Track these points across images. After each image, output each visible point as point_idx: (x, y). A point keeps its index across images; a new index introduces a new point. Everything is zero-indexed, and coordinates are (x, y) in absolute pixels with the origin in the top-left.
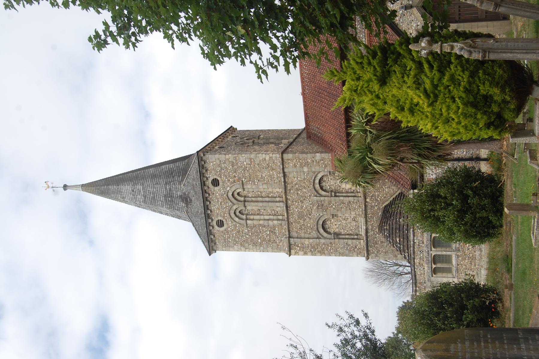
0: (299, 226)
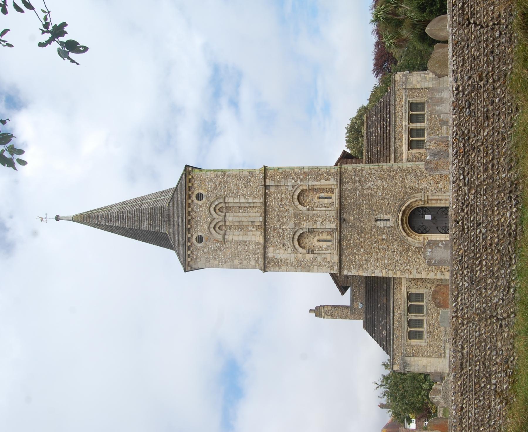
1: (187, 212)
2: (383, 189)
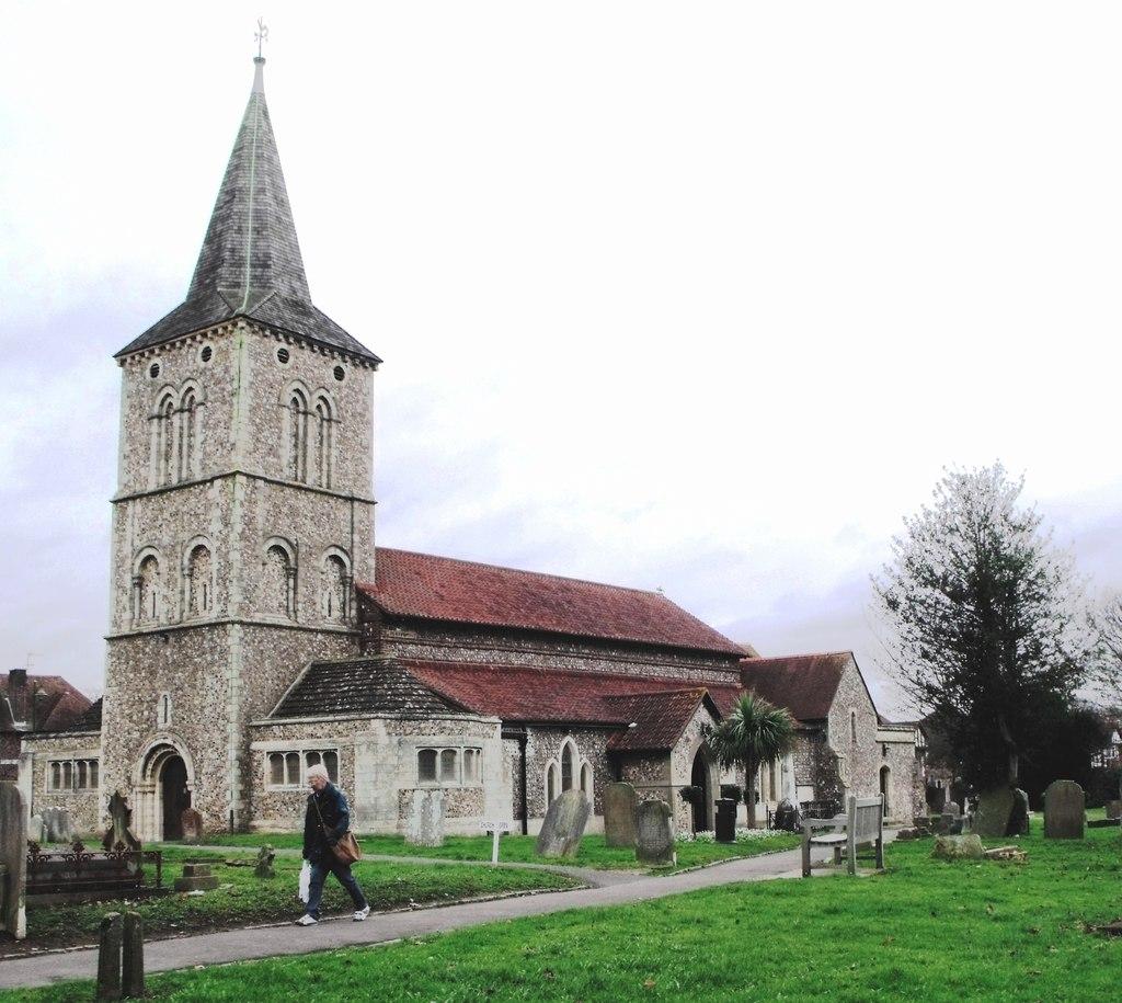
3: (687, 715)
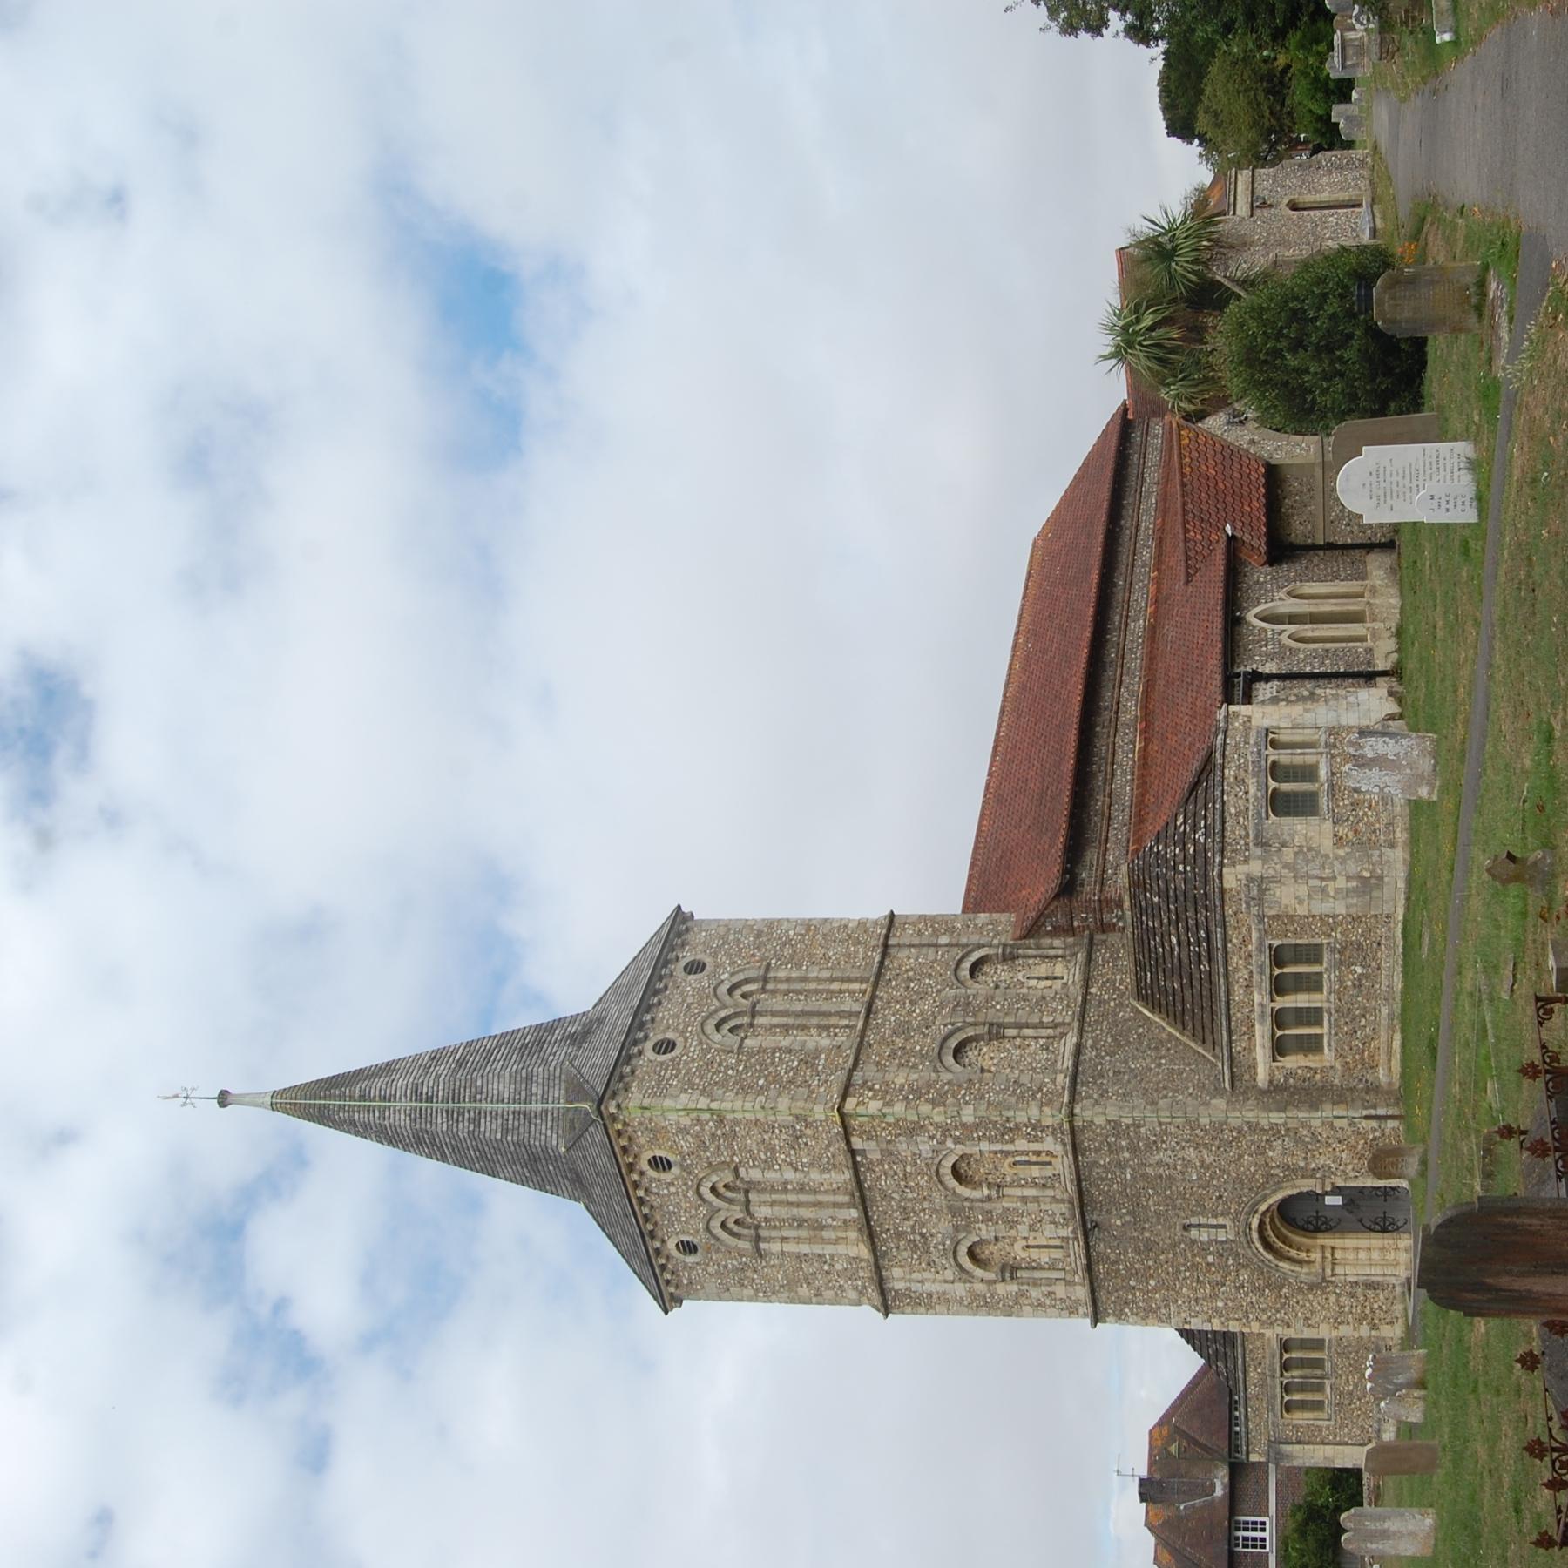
0: (889, 1050)
1: (634, 1201)
2: (1201, 1167)
3: (1210, 437)
